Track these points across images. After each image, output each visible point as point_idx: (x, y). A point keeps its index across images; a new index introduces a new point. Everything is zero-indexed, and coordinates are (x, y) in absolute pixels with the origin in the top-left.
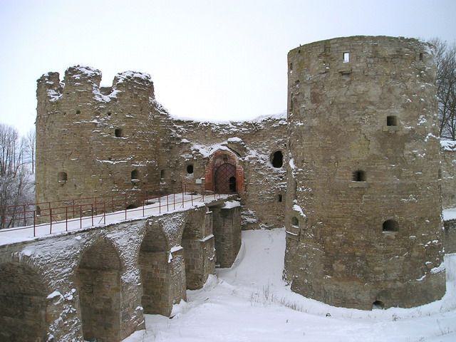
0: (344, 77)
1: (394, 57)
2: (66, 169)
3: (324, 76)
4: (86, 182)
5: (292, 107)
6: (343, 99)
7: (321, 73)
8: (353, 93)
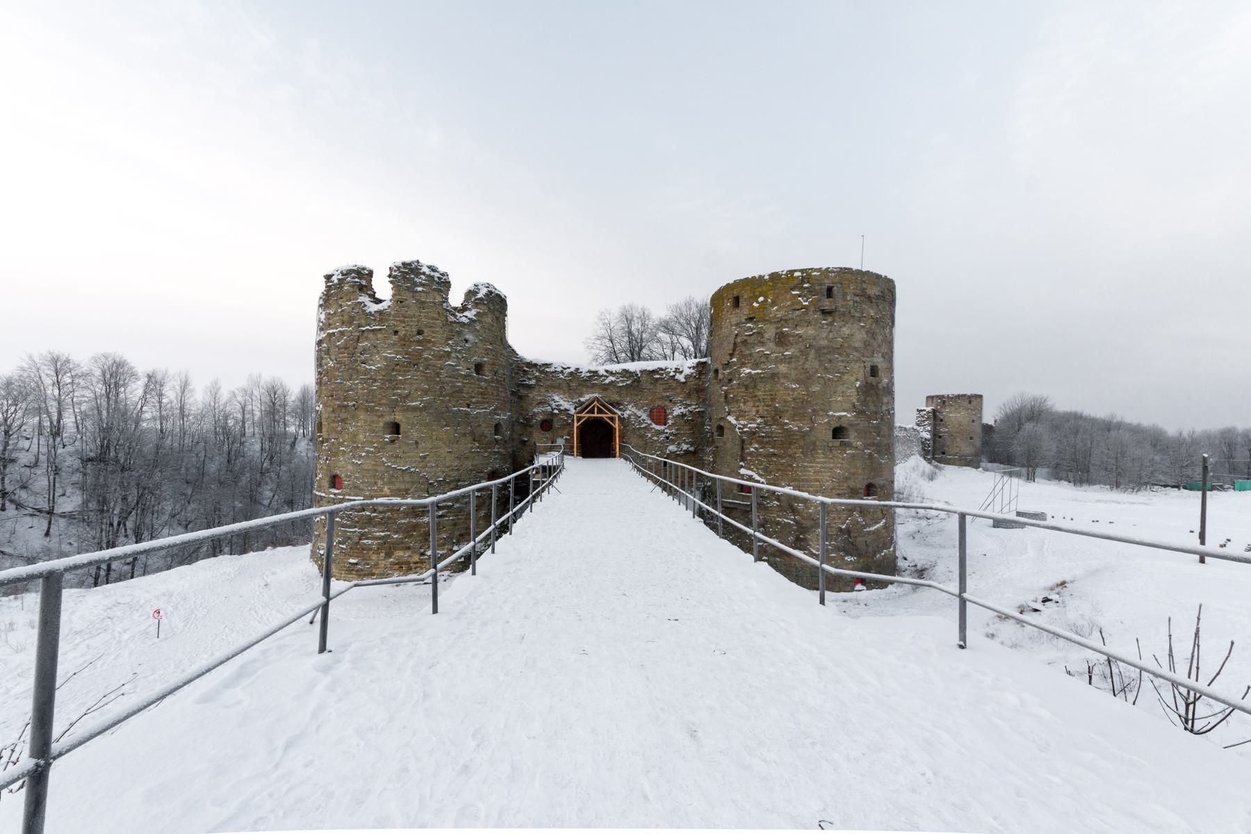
1: (878, 297)
2: (399, 417)
4: (434, 437)
5: (734, 350)
6: (824, 343)
7: (795, 310)
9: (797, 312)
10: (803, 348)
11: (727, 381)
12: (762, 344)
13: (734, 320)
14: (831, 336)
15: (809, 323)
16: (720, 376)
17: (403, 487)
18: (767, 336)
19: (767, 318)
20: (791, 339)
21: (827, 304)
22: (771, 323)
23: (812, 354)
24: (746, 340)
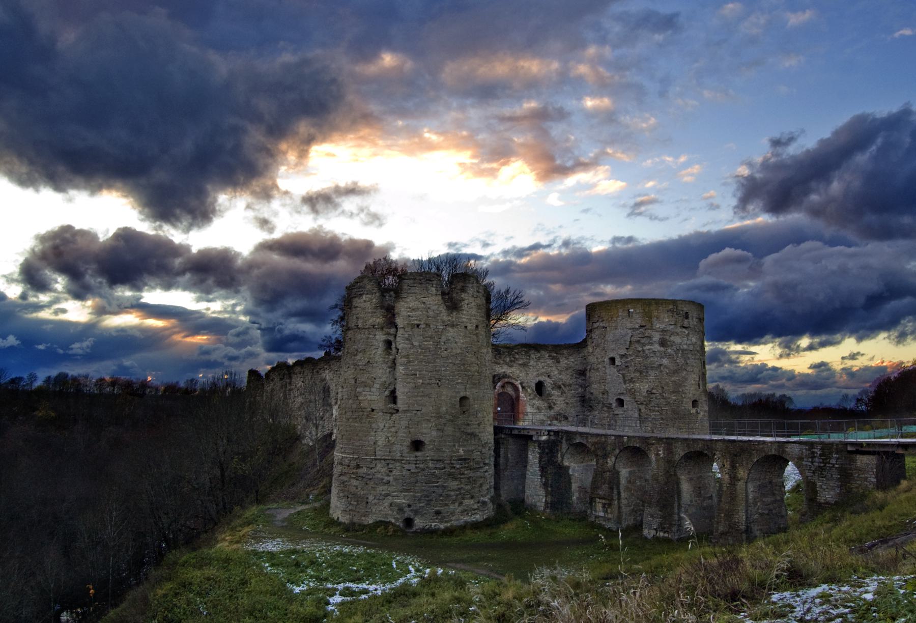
0: (684, 330)
3: (672, 327)
6: (685, 347)
8: (690, 343)
10: (675, 349)
11: (624, 367)
12: (651, 344)
13: (629, 325)
14: (688, 342)
15: (678, 334)
16: (618, 362)
17: (470, 449)
18: (654, 339)
19: (654, 328)
21: (686, 323)
22: (657, 331)
24: (639, 341)
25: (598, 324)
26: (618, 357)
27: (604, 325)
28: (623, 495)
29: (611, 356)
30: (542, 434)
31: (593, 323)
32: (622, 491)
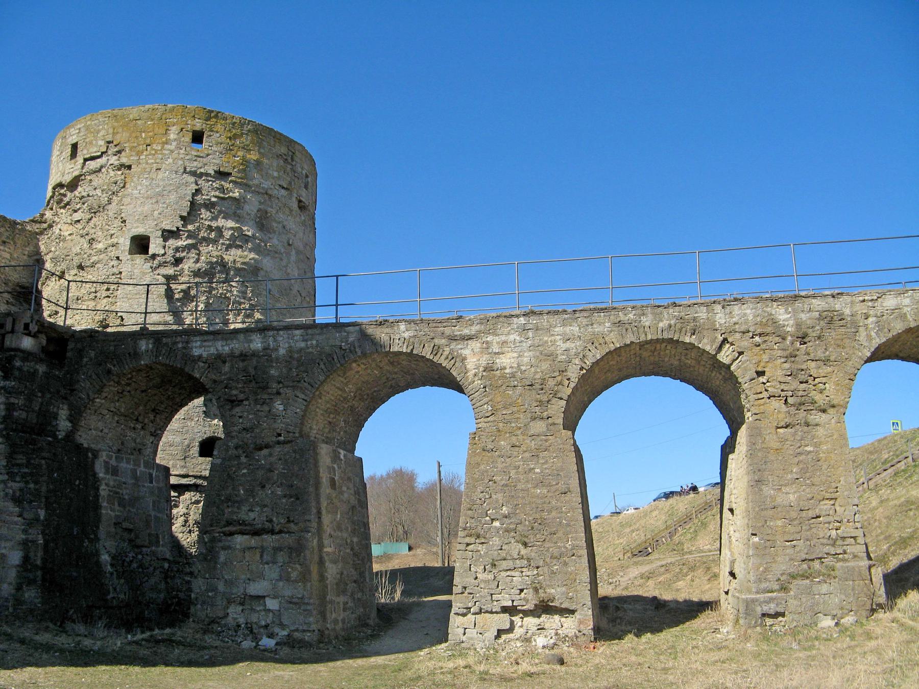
3: (283, 192)
9: (283, 191)
11: (169, 258)
20: (275, 225)
23: (293, 258)
25: (100, 162)
26: (160, 233)
27: (124, 160)
28: (326, 519)
29: (140, 230)
30: (20, 327)
31: (86, 160)
32: (324, 512)
